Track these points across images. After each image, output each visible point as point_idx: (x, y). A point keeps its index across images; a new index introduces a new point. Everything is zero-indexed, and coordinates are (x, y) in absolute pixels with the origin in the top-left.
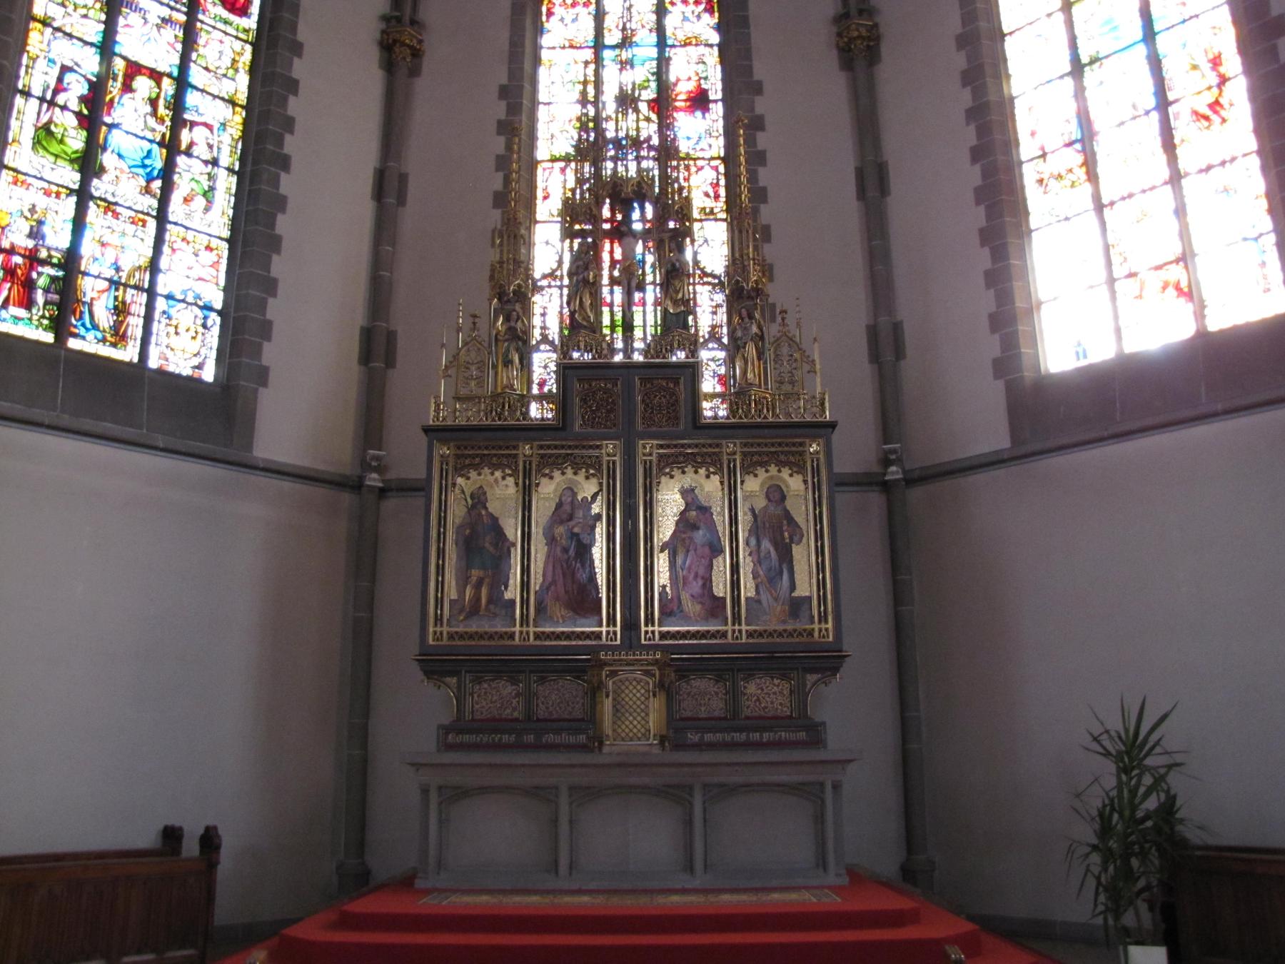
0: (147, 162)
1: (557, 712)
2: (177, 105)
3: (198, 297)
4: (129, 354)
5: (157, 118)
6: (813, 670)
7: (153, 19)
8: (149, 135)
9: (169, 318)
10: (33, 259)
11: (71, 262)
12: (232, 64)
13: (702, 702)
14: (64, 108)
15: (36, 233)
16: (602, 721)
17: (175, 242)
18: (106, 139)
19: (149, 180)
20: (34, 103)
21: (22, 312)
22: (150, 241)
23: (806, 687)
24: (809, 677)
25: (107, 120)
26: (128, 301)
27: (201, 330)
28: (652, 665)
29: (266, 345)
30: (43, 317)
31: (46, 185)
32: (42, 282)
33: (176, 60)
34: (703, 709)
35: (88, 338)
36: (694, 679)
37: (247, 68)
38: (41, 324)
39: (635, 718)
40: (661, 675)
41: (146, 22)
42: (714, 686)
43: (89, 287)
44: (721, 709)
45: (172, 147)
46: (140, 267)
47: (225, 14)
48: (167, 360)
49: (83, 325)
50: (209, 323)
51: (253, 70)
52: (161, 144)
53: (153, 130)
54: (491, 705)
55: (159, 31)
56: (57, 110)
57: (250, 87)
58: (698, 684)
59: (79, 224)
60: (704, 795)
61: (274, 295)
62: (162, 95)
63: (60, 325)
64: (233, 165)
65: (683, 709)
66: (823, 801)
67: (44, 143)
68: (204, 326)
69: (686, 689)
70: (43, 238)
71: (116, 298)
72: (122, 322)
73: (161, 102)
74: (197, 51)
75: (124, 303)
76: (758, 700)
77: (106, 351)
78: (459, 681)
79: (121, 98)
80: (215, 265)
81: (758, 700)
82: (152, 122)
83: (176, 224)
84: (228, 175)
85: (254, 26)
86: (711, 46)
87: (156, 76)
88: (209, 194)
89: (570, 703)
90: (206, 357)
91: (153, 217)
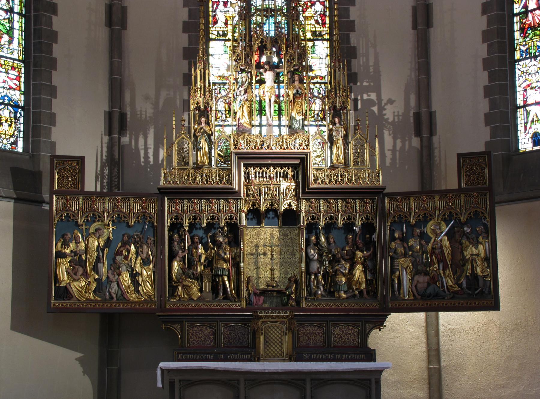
1: (234, 343)
6: (369, 322)
13: (311, 338)
16: (259, 347)
23: (366, 331)
24: (368, 325)
27: (13, 120)
28: (285, 318)
29: (53, 128)
34: (311, 342)
36: (307, 326)
39: (276, 346)
40: (289, 323)
42: (317, 330)
44: (321, 342)
54: (199, 339)
58: (309, 328)
60: (312, 384)
61: (55, 97)
64: (22, 10)
65: (301, 342)
66: (370, 388)
69: (303, 331)
76: (341, 337)
78: (182, 327)
80: (18, 78)
81: (341, 337)
84: (19, 18)
89: (241, 338)
90: (17, 137)
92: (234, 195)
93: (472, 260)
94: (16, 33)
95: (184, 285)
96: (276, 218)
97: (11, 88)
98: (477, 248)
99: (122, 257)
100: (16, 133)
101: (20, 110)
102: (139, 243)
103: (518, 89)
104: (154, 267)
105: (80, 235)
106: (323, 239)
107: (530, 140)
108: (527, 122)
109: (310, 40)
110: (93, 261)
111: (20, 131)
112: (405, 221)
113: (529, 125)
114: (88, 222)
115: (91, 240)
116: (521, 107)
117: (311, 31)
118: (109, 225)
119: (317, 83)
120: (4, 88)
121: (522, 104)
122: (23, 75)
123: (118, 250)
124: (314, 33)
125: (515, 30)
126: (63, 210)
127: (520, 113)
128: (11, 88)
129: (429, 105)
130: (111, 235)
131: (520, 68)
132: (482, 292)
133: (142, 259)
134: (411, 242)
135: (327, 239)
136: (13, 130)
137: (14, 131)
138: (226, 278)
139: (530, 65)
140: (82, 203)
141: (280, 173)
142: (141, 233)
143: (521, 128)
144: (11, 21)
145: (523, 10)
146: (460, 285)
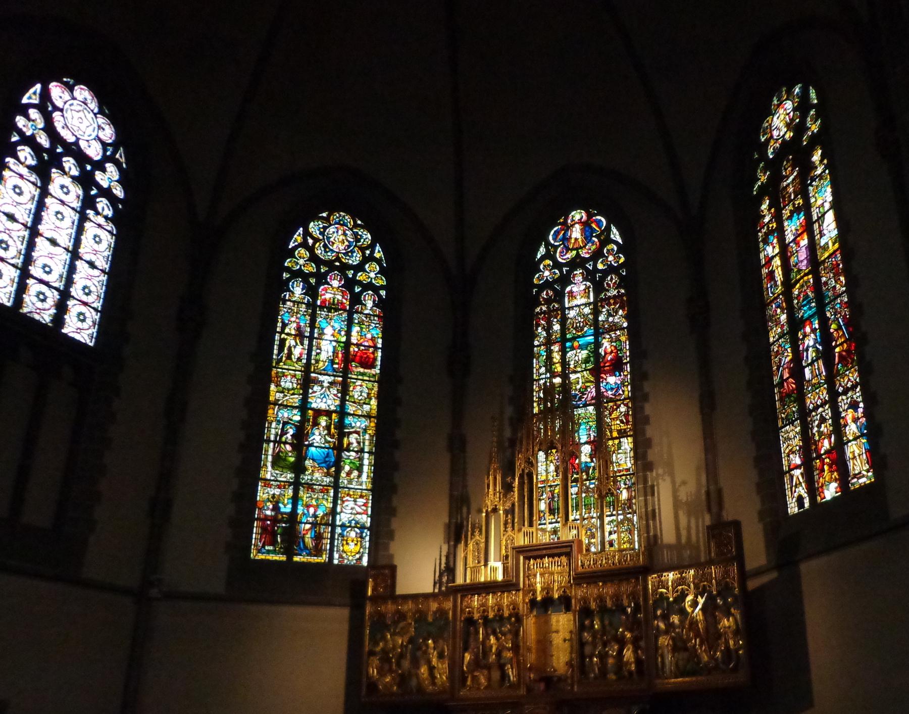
0: (327, 459)
2: (341, 426)
3: (357, 523)
4: (324, 558)
7: (326, 384)
8: (327, 445)
9: (343, 536)
10: (274, 520)
12: (368, 396)
15: (276, 508)
17: (344, 497)
18: (306, 453)
19: (328, 468)
20: (271, 445)
21: (271, 548)
22: (330, 499)
25: (306, 443)
26: (322, 531)
27: (359, 539)
30: (281, 548)
31: (279, 483)
32: (279, 531)
33: (338, 402)
37: (376, 396)
38: (280, 551)
41: (322, 387)
45: (339, 448)
46: (327, 514)
47: (362, 370)
48: (342, 558)
49: (300, 548)
50: (364, 535)
51: (379, 397)
52: (333, 449)
53: (329, 442)
55: (329, 390)
56: (282, 445)
57: (378, 406)
59: (295, 499)
62: (333, 423)
63: (289, 552)
64: (372, 449)
68: (361, 537)
70: (279, 508)
71: (315, 532)
72: (319, 543)
73: (332, 426)
74: (348, 394)
75: (320, 533)
79: (312, 429)
80: (365, 505)
82: (329, 439)
83: (344, 488)
85: (378, 372)
87: (328, 413)
88: (360, 469)
91: (331, 486)
94: (366, 469)
97: (358, 513)
101: (366, 531)
109: (616, 438)
111: (365, 548)
114: (396, 623)
117: (617, 430)
119: (623, 475)
120: (351, 513)
122: (370, 501)
124: (619, 431)
128: (358, 513)
129: (716, 483)
144: (361, 459)
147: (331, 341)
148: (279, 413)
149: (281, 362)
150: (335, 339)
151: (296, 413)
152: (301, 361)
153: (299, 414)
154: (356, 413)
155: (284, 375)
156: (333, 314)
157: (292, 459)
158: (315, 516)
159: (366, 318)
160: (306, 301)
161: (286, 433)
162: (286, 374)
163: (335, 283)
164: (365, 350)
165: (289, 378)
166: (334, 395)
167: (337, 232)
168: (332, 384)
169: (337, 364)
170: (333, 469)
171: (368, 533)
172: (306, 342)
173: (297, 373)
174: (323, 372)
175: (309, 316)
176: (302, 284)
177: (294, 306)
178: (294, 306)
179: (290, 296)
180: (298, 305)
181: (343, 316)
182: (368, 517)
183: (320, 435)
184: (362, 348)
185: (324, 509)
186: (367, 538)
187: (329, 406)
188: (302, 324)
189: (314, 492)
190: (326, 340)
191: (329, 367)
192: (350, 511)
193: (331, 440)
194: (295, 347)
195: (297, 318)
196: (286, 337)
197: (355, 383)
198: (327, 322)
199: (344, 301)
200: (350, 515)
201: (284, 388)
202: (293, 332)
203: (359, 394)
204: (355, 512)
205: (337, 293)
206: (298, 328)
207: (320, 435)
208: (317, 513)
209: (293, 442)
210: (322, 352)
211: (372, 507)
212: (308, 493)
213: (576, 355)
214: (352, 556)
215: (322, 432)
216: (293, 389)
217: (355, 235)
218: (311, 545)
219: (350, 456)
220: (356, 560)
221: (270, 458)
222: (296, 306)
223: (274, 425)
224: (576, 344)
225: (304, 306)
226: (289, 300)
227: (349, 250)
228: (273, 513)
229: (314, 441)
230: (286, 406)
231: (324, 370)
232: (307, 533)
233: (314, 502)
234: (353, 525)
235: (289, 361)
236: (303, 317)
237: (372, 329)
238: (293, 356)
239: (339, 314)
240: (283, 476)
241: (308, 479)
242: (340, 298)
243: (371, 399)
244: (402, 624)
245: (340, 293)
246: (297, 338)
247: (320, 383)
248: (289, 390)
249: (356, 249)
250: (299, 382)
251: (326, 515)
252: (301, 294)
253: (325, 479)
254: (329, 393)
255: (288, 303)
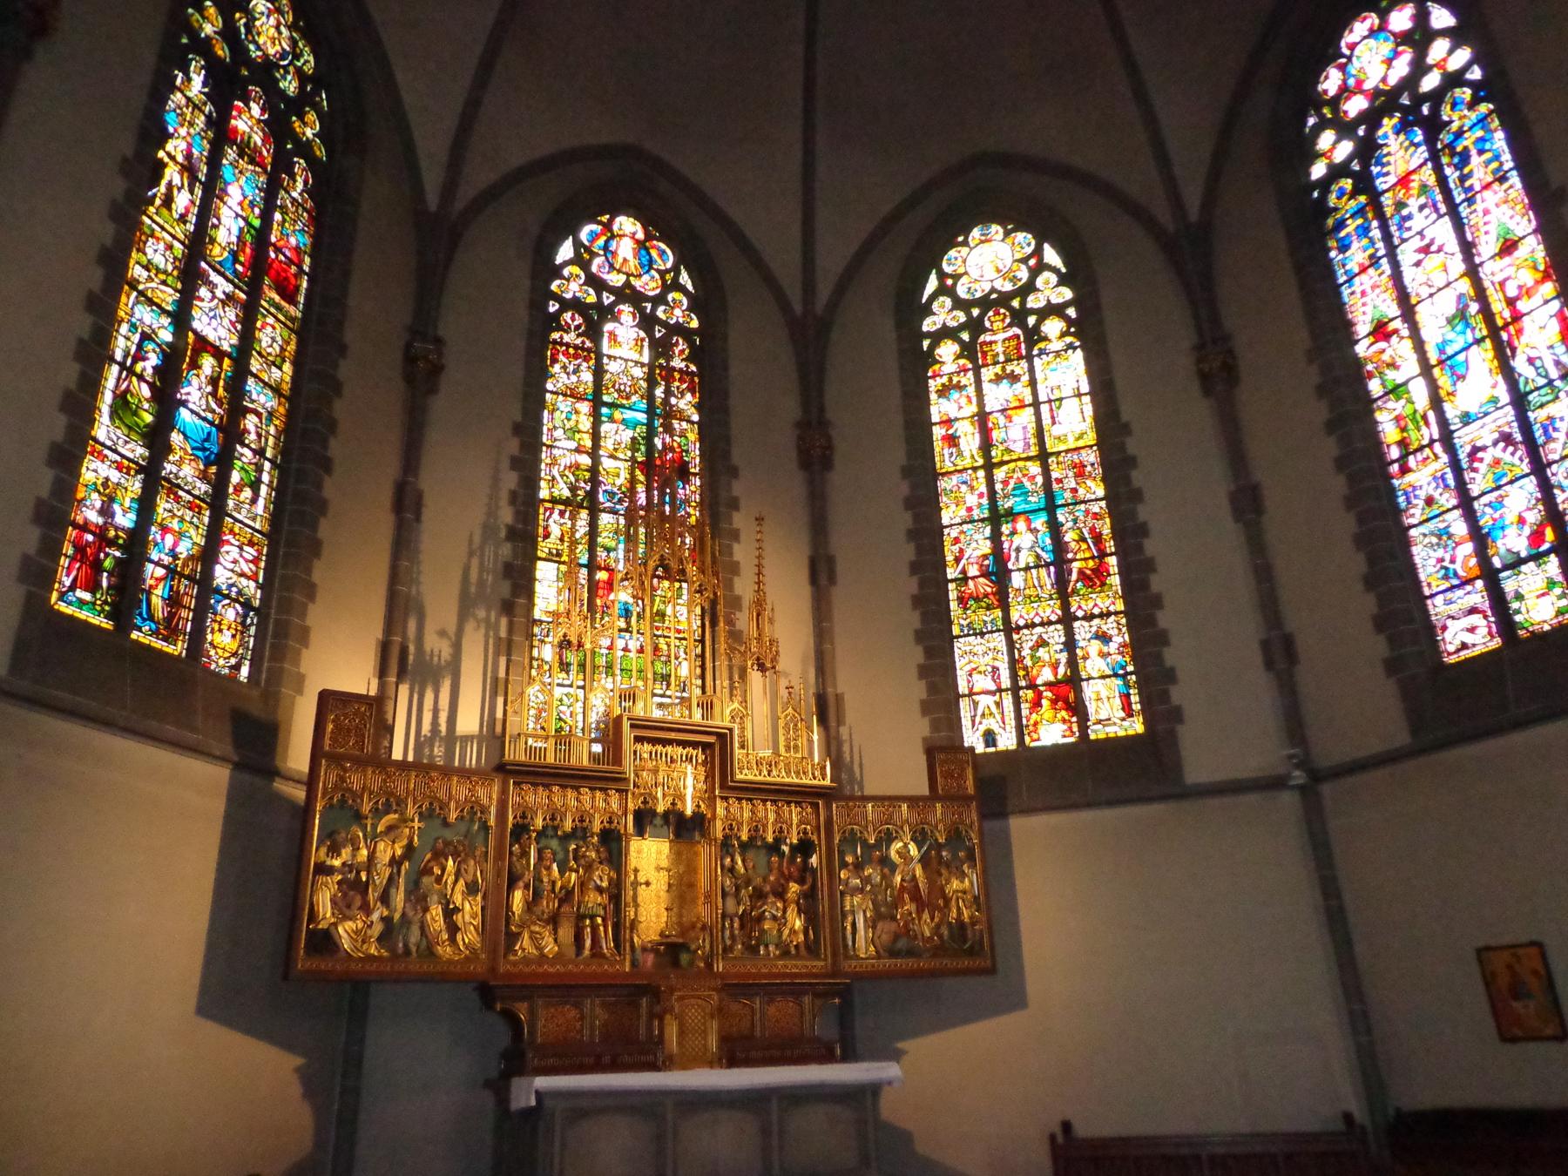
0: (206, 445)
3: (240, 593)
5: (216, 399)
8: (209, 416)
11: (136, 543)
12: (281, 352)
14: (141, 378)
19: (208, 464)
33: (234, 341)
35: (143, 629)
38: (103, 611)
43: (152, 572)
45: (230, 432)
47: (277, 298)
50: (249, 621)
52: (219, 428)
53: (213, 411)
55: (223, 308)
56: (134, 379)
59: (145, 506)
62: (223, 376)
67: (120, 412)
70: (113, 515)
73: (221, 383)
75: (178, 592)
76: (777, 1021)
77: (158, 644)
80: (255, 561)
82: (214, 406)
86: (692, 423)
87: (218, 354)
88: (255, 485)
90: (242, 658)
92: (620, 784)
93: (957, 899)
94: (264, 490)
95: (532, 932)
96: (666, 827)
97: (242, 575)
98: (962, 882)
99: (433, 878)
100: (241, 651)
102: (463, 855)
103: (959, 672)
104: (484, 898)
105: (361, 835)
106: (740, 862)
107: (981, 739)
108: (975, 716)
110: (381, 883)
111: (248, 648)
112: (860, 838)
113: (978, 719)
114: (378, 813)
115: (381, 846)
116: (965, 696)
118: (413, 821)
120: (232, 571)
121: (967, 692)
122: (264, 558)
123: (425, 866)
125: (951, 598)
126: (336, 787)
127: (964, 704)
128: (242, 575)
130: (416, 838)
131: (960, 646)
132: (972, 947)
133: (466, 884)
134: (868, 871)
135: (744, 861)
136: (236, 645)
137: (239, 646)
138: (599, 920)
139: (975, 642)
140: (374, 780)
141: (682, 756)
142: (466, 836)
143: (966, 722)
144: (259, 469)
145: (960, 576)
146: (941, 937)
147: (237, 215)
148: (136, 309)
149: (152, 204)
150: (244, 214)
151: (166, 325)
152: (185, 223)
153: (171, 329)
154: (259, 374)
155: (152, 236)
156: (245, 166)
157: (148, 418)
158: (175, 557)
159: (293, 205)
160: (207, 110)
161: (144, 359)
162: (157, 234)
163: (256, 109)
164: (285, 263)
165: (161, 246)
166: (231, 321)
167: (268, 17)
168: (229, 299)
169: (242, 264)
170: (213, 469)
171: (255, 621)
172: (198, 191)
173: (177, 245)
174: (218, 267)
175: (209, 142)
176: (203, 72)
177: (187, 108)
178: (187, 108)
179: (183, 82)
180: (193, 110)
181: (261, 179)
182: (257, 587)
183: (200, 389)
184: (282, 257)
185: (190, 546)
186: (253, 630)
187: (220, 339)
188: (195, 152)
189: (178, 503)
190: (230, 208)
191: (229, 265)
192: (231, 566)
193: (218, 410)
194: (179, 189)
195: (188, 133)
196: (166, 159)
197: (265, 316)
198: (234, 175)
199: (265, 153)
200: (230, 574)
201: (149, 261)
202: (180, 158)
203: (270, 342)
204: (239, 571)
205: (255, 129)
206: (189, 155)
207: (200, 389)
208: (178, 550)
209: (154, 382)
210: (221, 227)
211: (265, 569)
212: (167, 501)
213: (616, 433)
214: (225, 659)
215: (204, 386)
216: (165, 272)
217: (294, 43)
218: (161, 615)
219: (242, 455)
220: (231, 667)
221: (108, 397)
222: (190, 109)
223: (124, 328)
224: (617, 415)
225: (203, 118)
226: (182, 92)
227: (282, 63)
228: (100, 521)
229: (189, 397)
230: (150, 302)
231: (220, 263)
232: (157, 586)
233: (175, 525)
234: (233, 595)
235: (164, 211)
236: (197, 138)
237: (299, 231)
238: (174, 206)
239: (254, 171)
240: (128, 446)
241: (171, 473)
242: (259, 143)
243: (284, 361)
244: (392, 817)
245: (261, 134)
246: (186, 175)
247: (212, 287)
248: (158, 271)
249: (291, 69)
250: (177, 263)
251: (191, 558)
252: (201, 92)
253: (199, 483)
254: (222, 314)
255: (179, 95)
